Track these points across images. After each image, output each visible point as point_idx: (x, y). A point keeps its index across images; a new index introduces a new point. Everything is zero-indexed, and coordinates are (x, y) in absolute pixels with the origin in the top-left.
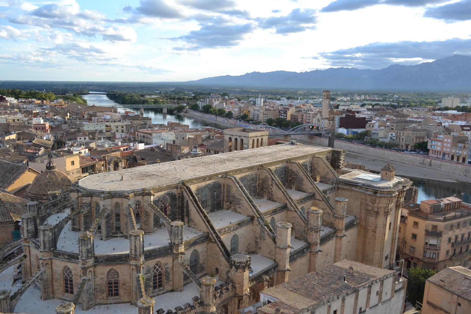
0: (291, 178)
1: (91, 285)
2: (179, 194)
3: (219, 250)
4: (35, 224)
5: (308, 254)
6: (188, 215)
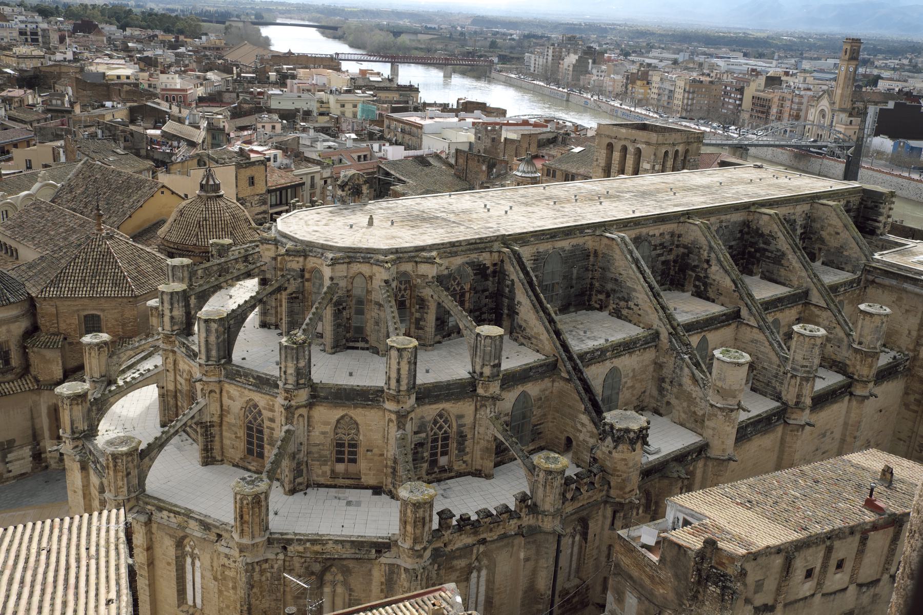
1: (301, 444)
2: (495, 265)
3: (578, 398)
4: (187, 305)
5: (780, 430)
6: (513, 313)
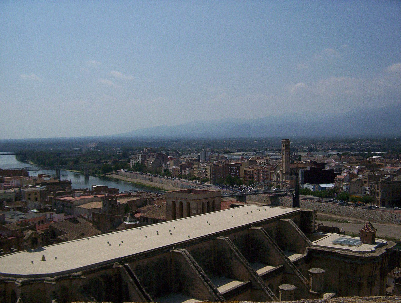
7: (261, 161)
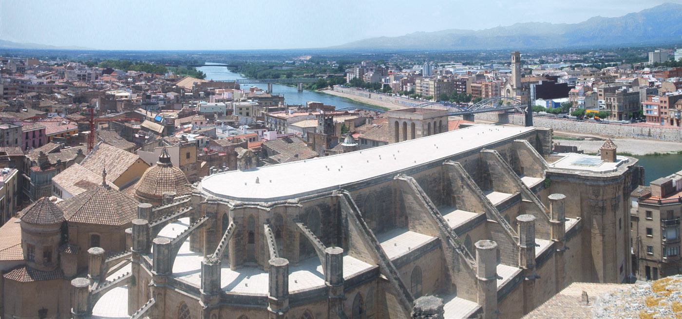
0: (486, 175)
4: (148, 234)
7: (489, 75)
